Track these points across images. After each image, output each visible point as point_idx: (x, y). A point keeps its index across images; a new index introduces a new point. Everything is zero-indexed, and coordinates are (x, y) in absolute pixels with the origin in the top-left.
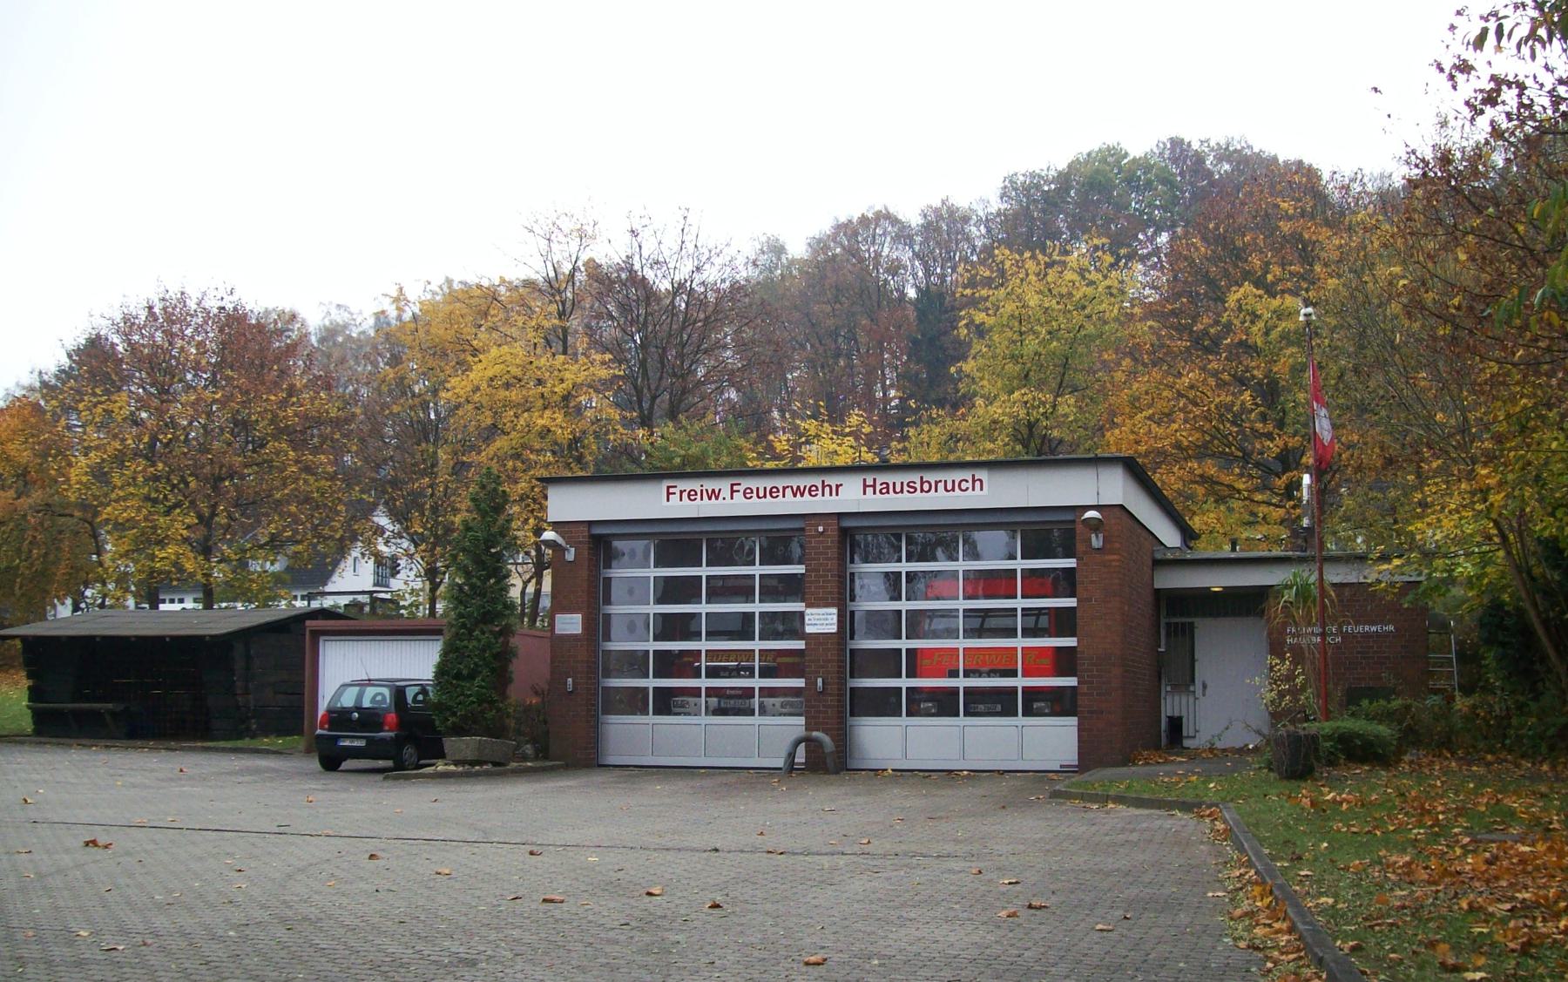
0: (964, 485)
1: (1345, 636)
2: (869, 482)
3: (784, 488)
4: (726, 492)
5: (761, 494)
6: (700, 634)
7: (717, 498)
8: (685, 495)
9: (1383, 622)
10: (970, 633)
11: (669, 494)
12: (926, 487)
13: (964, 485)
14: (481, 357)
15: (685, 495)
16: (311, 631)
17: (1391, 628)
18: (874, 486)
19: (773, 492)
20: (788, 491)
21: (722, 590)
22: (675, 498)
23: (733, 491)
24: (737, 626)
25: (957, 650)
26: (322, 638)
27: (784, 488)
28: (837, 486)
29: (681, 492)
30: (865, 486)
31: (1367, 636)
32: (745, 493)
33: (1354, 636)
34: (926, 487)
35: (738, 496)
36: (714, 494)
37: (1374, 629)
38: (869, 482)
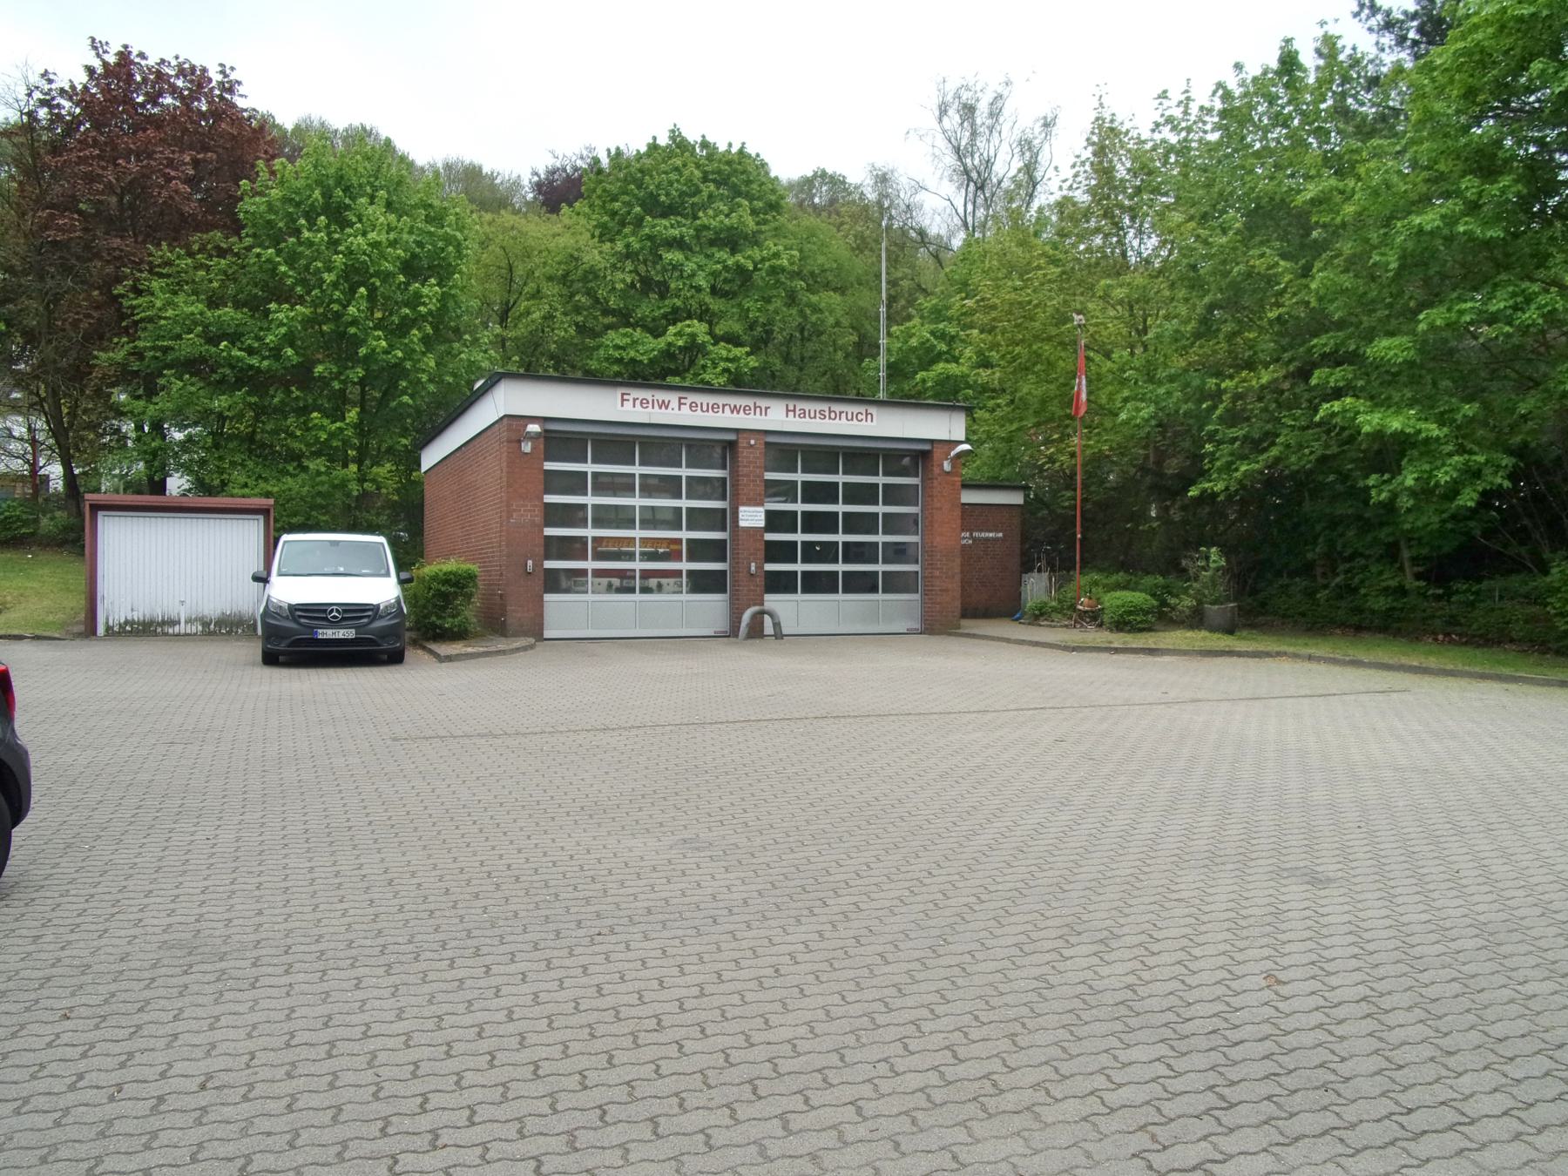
0: (860, 417)
1: (974, 539)
2: (791, 408)
3: (724, 406)
4: (674, 404)
5: (705, 408)
6: (634, 521)
7: (667, 408)
8: (638, 402)
9: (997, 531)
10: (582, 541)
11: (623, 400)
12: (833, 415)
13: (860, 417)
14: (596, 240)
15: (638, 402)
16: (91, 505)
17: (1000, 535)
18: (794, 411)
19: (714, 407)
20: (727, 408)
21: (604, 484)
22: (628, 405)
23: (680, 404)
24: (669, 516)
25: (796, 542)
26: (100, 514)
27: (724, 406)
28: (767, 408)
29: (635, 400)
30: (788, 411)
31: (987, 539)
32: (691, 406)
33: (980, 539)
34: (833, 415)
35: (686, 409)
36: (664, 405)
37: (991, 535)
38: (791, 408)
